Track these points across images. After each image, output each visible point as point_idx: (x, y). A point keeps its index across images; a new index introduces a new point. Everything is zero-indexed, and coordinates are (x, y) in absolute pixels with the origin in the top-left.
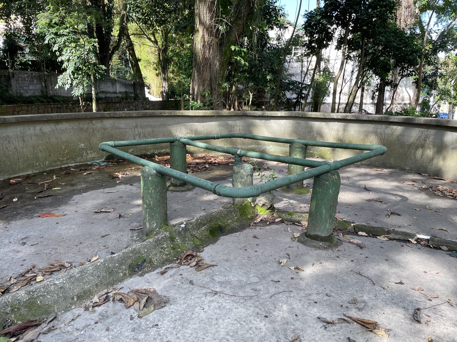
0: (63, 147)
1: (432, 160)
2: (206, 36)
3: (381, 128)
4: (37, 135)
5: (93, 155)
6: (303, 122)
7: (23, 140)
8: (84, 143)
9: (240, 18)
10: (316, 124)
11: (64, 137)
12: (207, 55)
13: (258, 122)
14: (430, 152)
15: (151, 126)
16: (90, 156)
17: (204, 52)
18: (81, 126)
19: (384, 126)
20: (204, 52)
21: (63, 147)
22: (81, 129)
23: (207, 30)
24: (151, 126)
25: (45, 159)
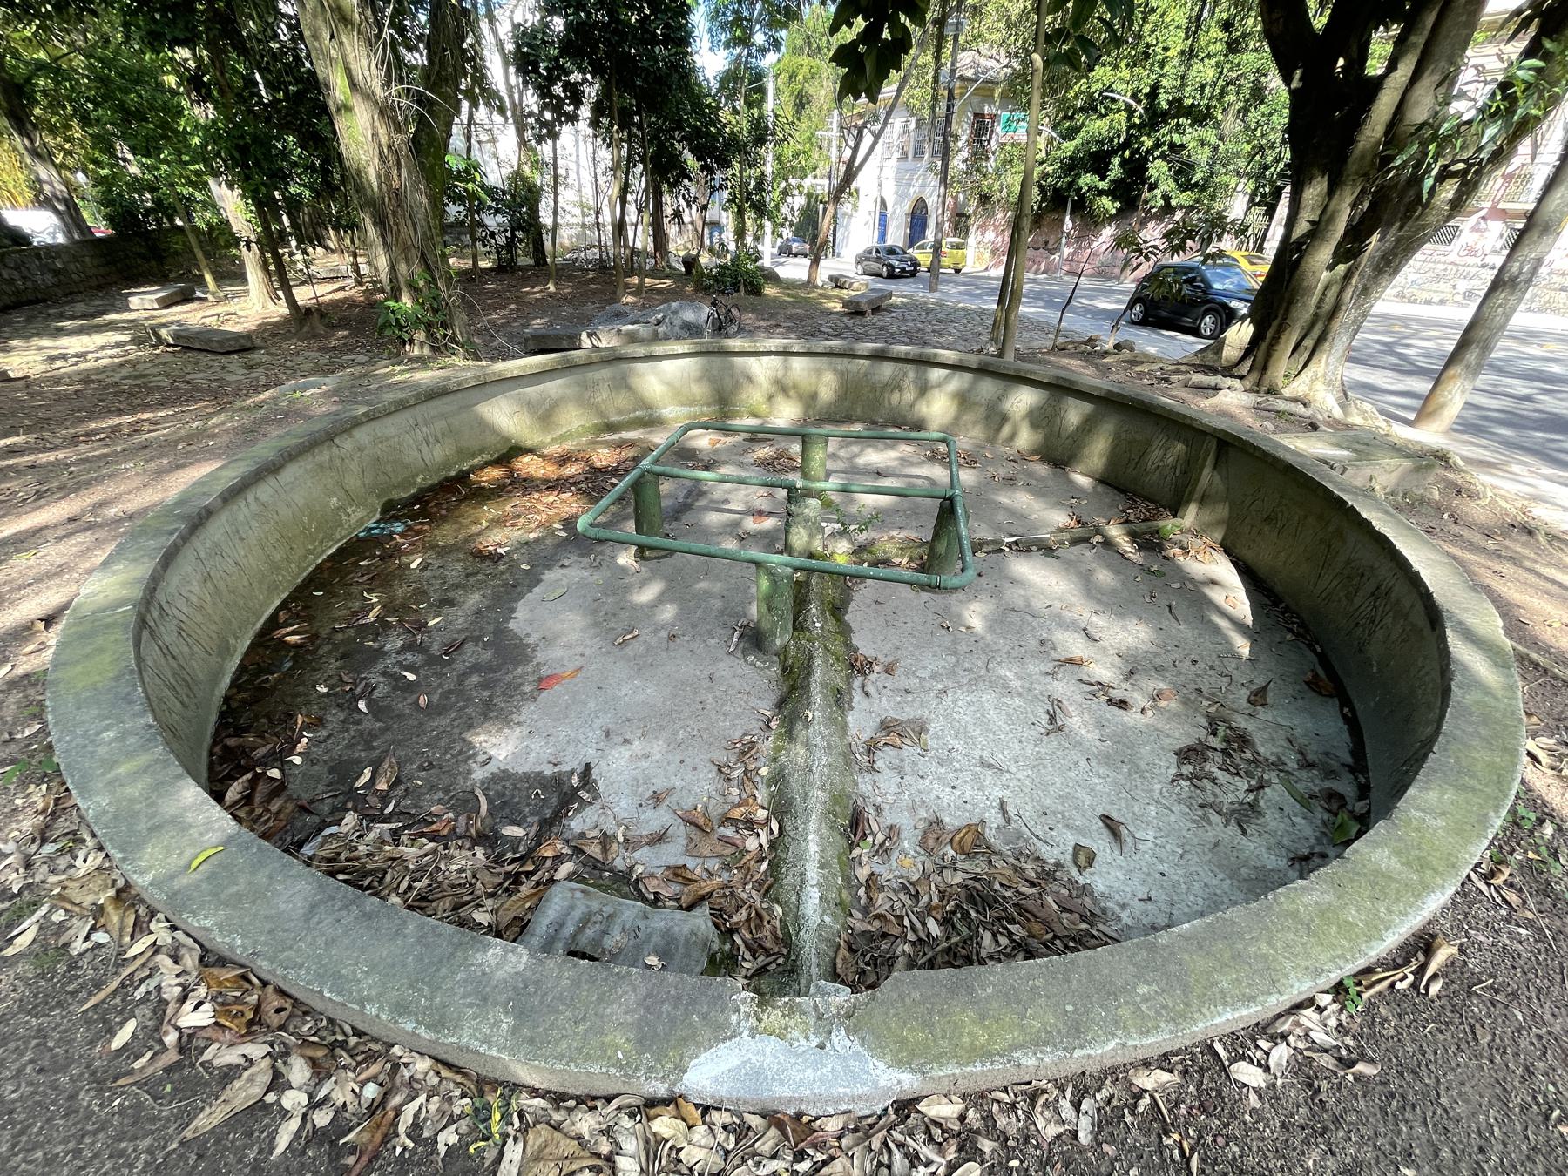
0: (305, 519)
1: (912, 406)
2: (382, 131)
3: (842, 363)
4: (256, 516)
5: (360, 513)
6: (717, 360)
7: (242, 539)
8: (335, 494)
9: (446, 80)
10: (738, 360)
11: (299, 498)
12: (396, 183)
13: (640, 366)
14: (909, 396)
15: (442, 416)
16: (354, 519)
17: (388, 176)
18: (319, 459)
19: (846, 360)
20: (388, 176)
21: (305, 519)
22: (321, 466)
23: (382, 114)
24: (442, 416)
25: (288, 560)
